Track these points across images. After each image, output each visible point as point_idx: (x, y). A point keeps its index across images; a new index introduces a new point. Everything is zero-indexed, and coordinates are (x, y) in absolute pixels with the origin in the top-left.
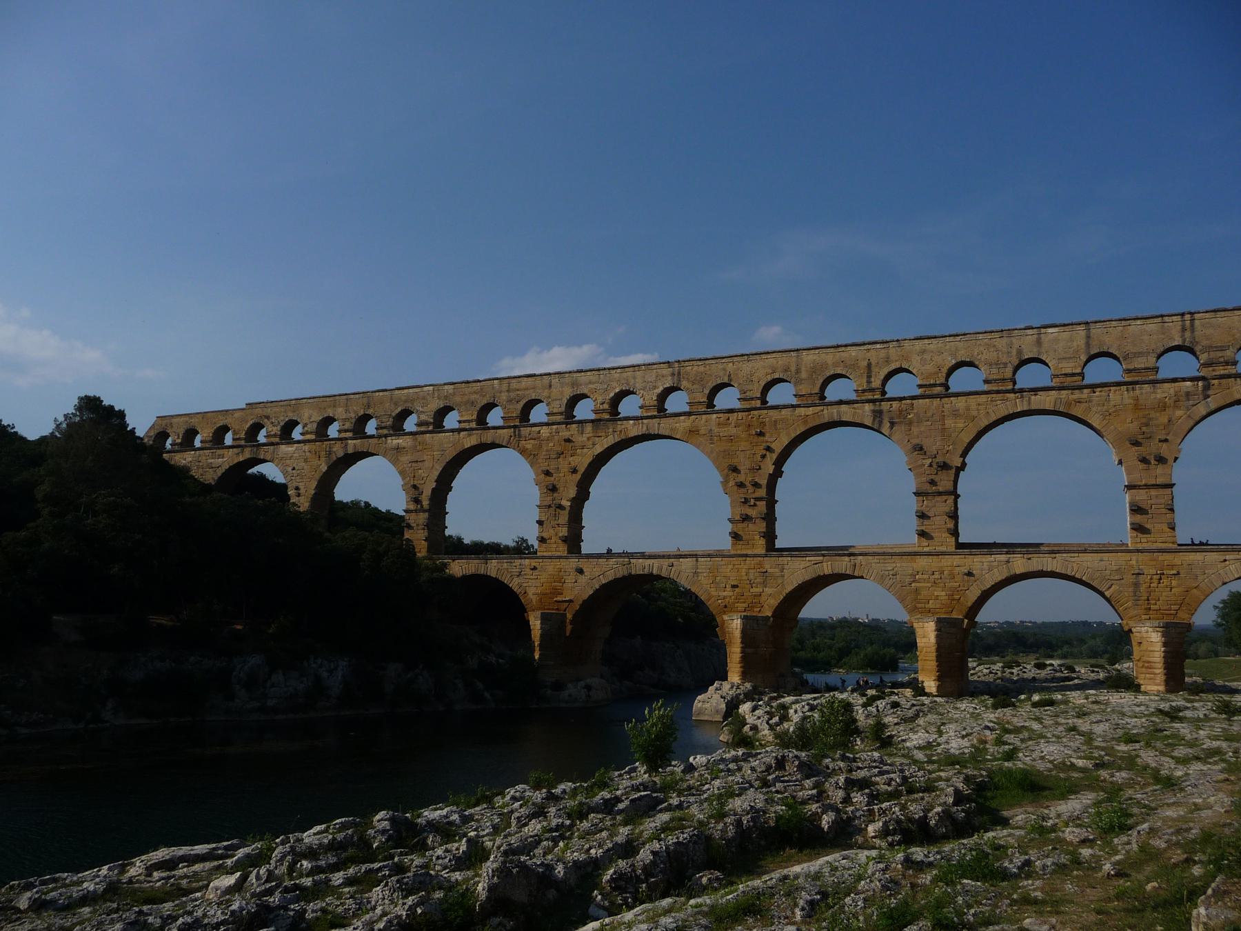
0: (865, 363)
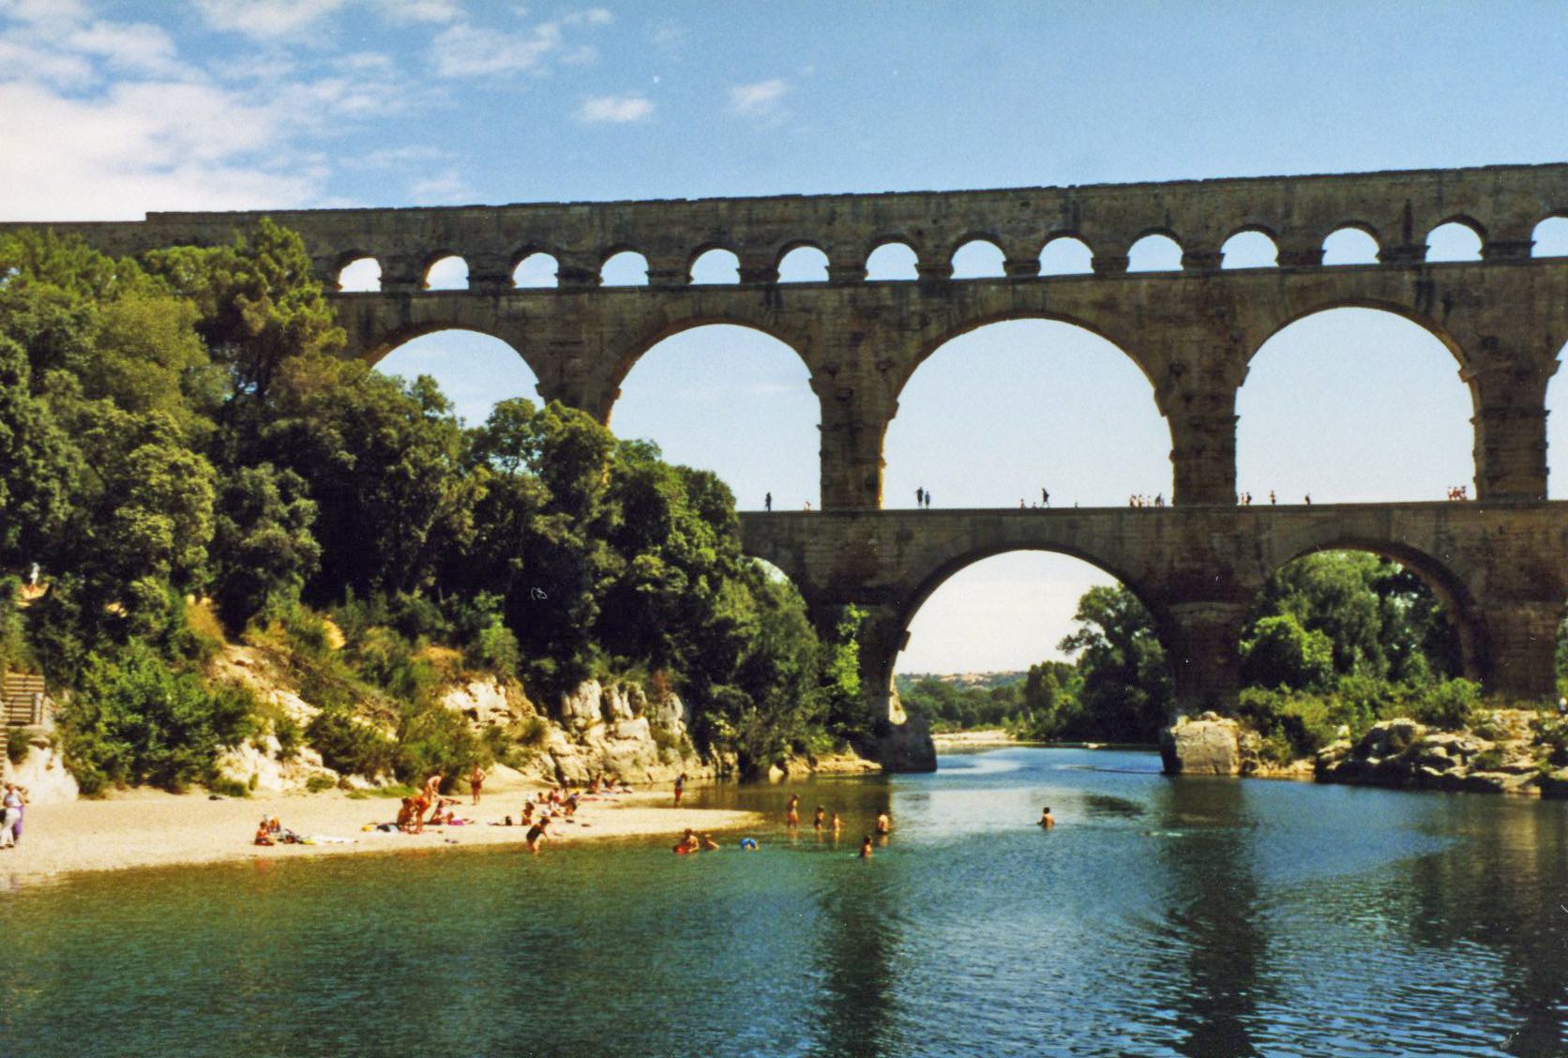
0: (1398, 207)
